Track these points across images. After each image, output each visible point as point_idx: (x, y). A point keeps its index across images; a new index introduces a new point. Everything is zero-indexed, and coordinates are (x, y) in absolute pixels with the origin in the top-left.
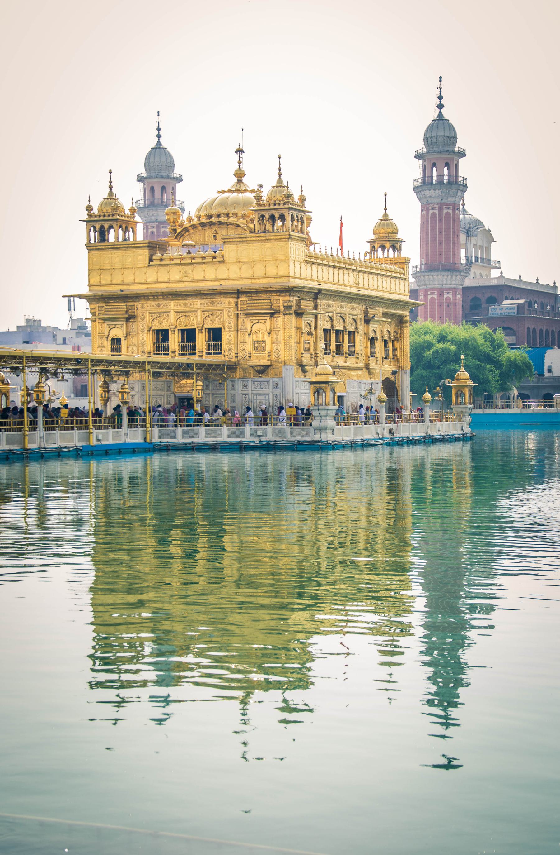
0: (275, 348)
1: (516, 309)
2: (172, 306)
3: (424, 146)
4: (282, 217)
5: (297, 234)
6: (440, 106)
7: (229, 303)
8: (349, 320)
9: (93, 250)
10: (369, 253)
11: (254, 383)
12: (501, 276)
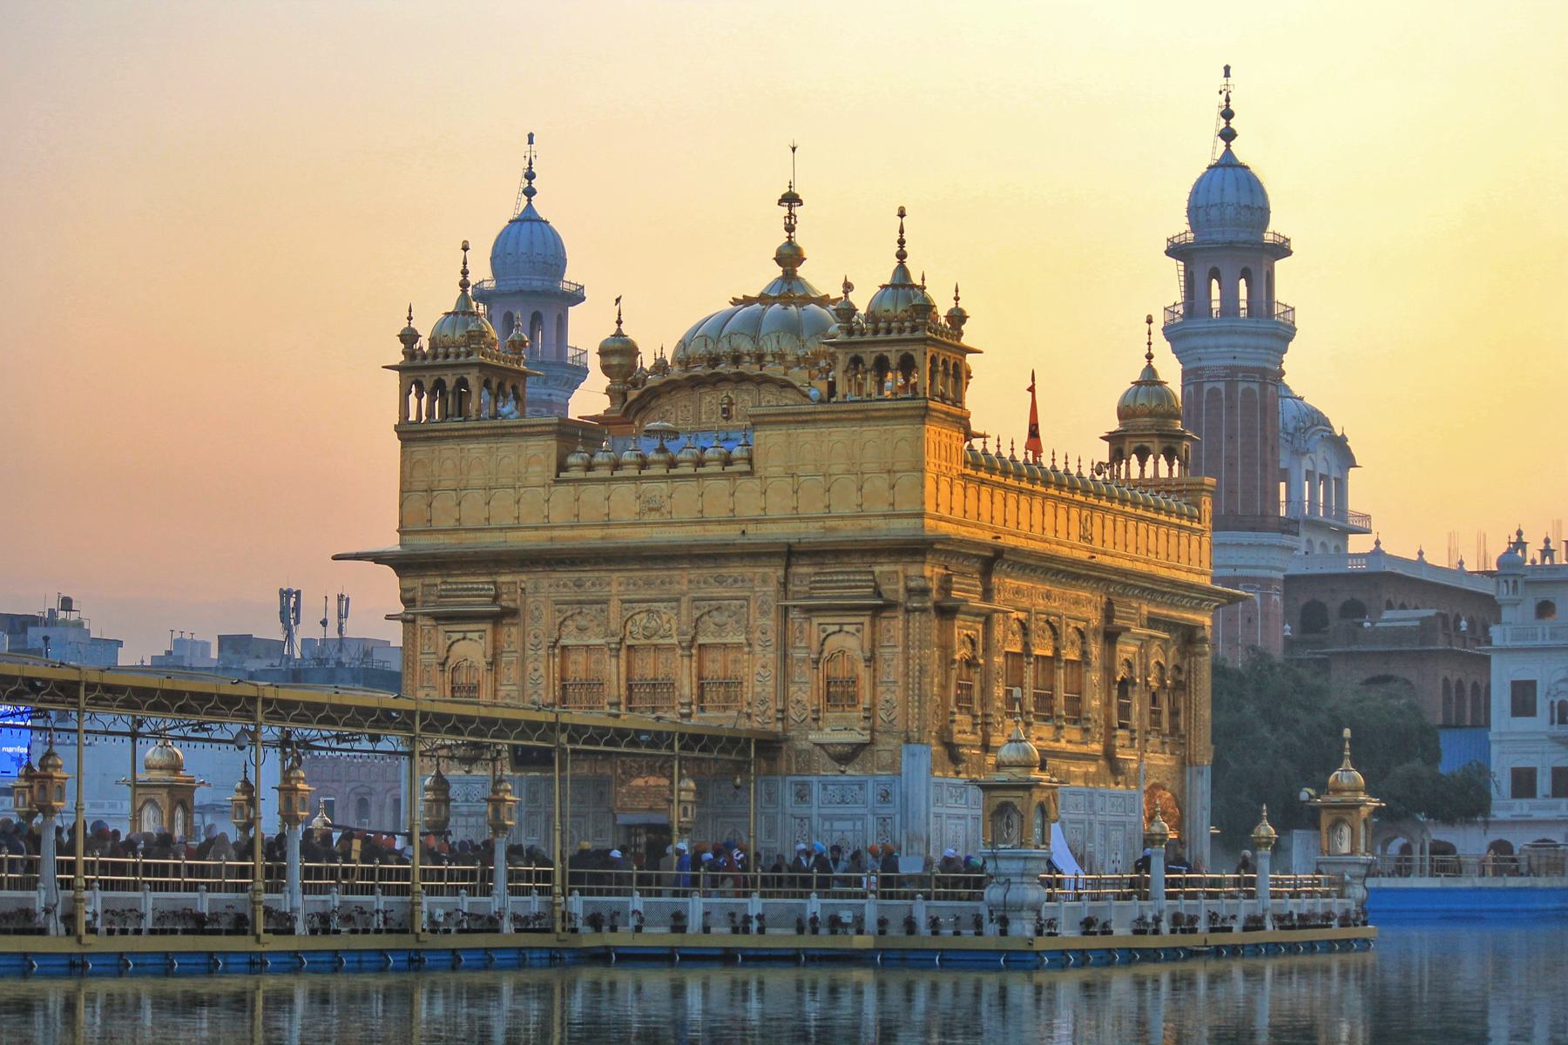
3: (1188, 228)
4: (907, 365)
5: (944, 407)
6: (1228, 135)
8: (1068, 632)
9: (414, 440)
10: (1107, 466)
11: (825, 789)
12: (1377, 552)
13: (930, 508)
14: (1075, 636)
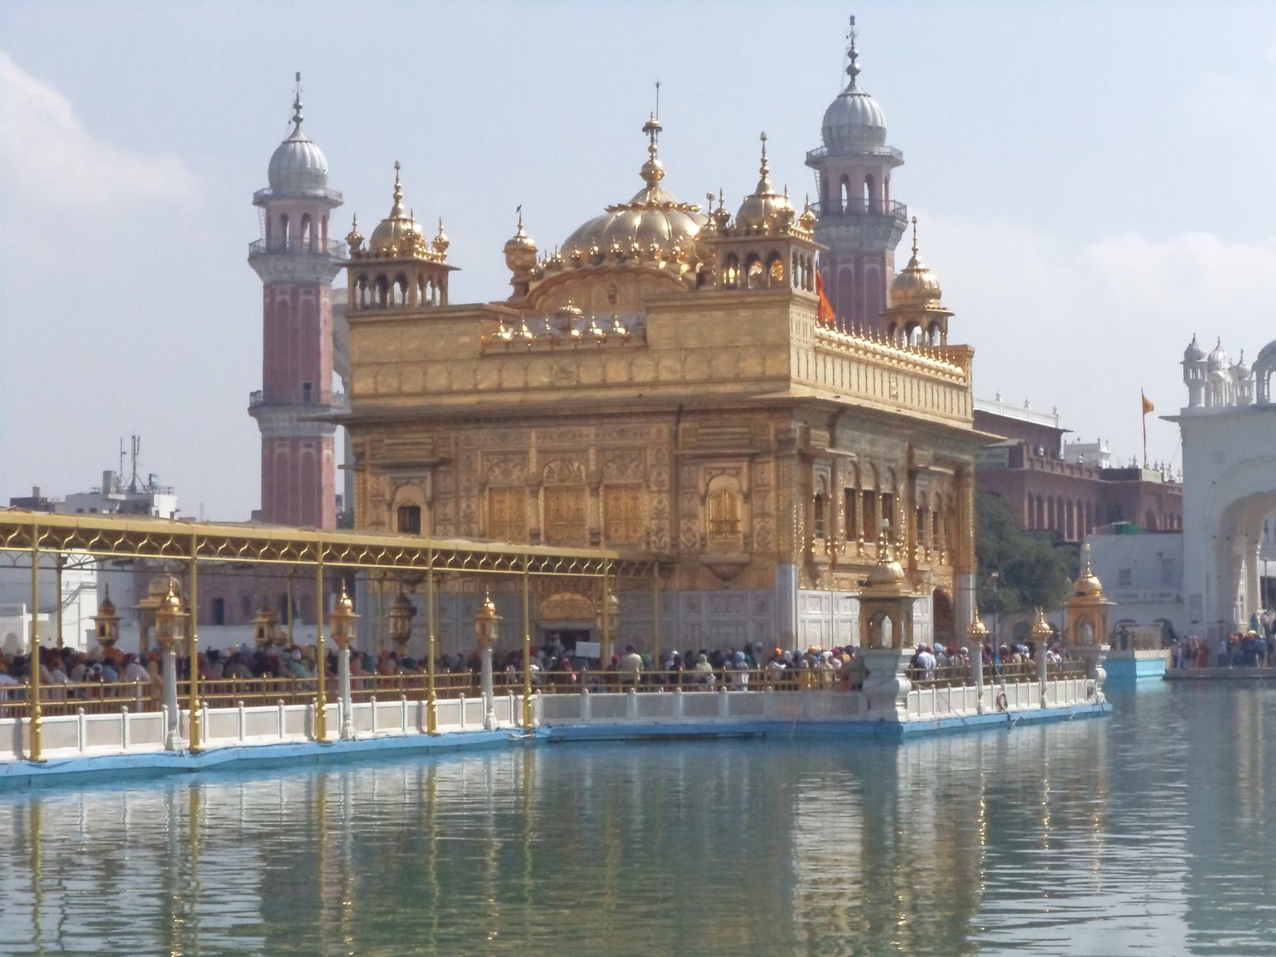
0: (758, 527)
1: (1007, 456)
2: (533, 437)
3: (822, 143)
7: (659, 432)
13: (794, 374)
14: (888, 475)
